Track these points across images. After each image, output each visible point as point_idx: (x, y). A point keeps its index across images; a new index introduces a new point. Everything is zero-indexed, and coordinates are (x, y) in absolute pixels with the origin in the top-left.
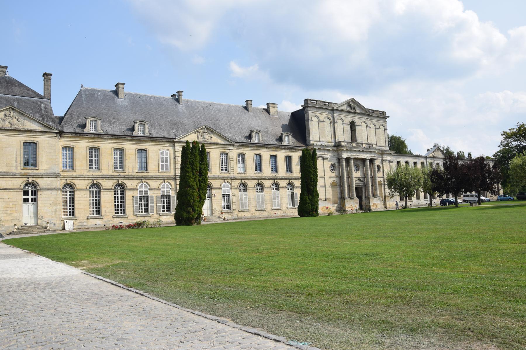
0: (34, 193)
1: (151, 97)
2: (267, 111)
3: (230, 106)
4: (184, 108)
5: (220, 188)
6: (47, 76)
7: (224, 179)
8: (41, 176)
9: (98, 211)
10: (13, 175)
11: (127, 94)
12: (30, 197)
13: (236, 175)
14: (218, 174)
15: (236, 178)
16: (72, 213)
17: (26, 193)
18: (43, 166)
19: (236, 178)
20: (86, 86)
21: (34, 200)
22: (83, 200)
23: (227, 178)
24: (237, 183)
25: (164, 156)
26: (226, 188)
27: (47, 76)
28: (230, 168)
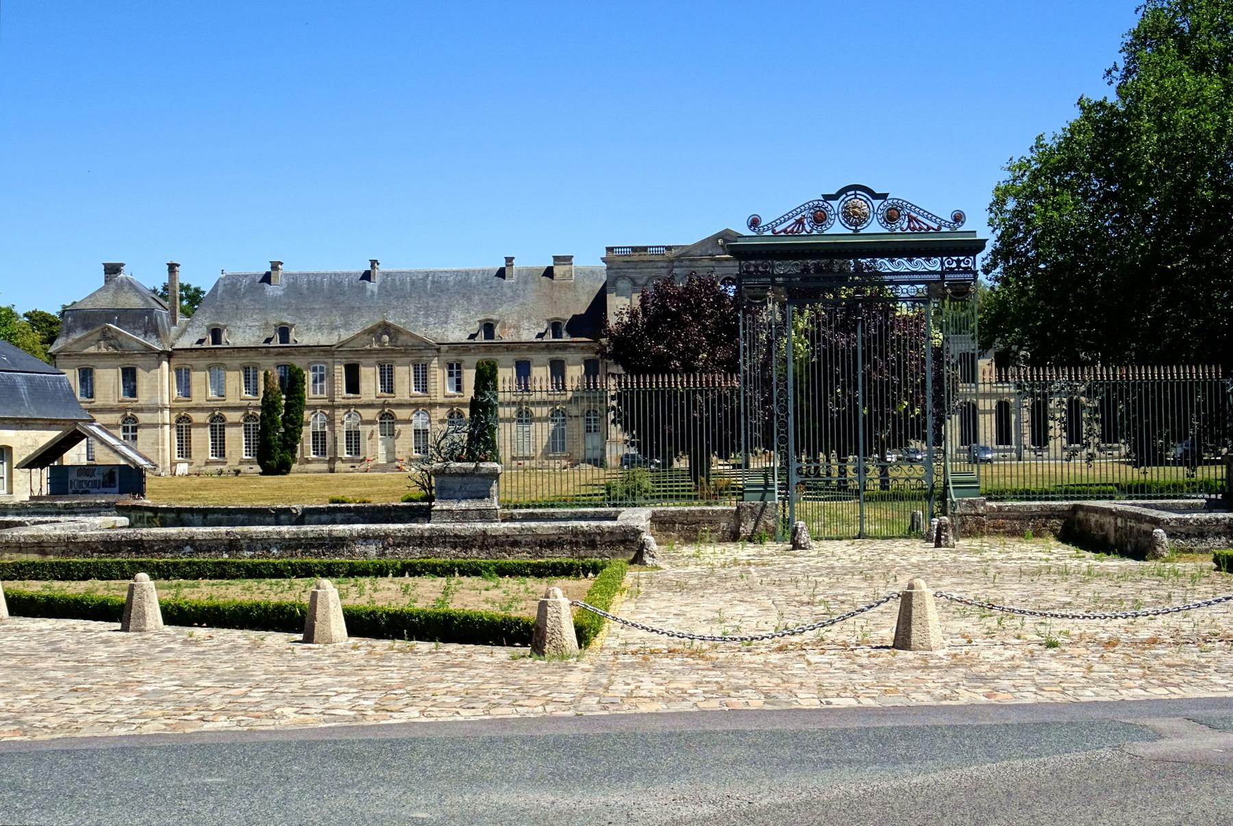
0: (135, 429)
1: (324, 275)
2: (549, 272)
3: (467, 273)
4: (376, 290)
5: (410, 421)
6: (172, 268)
7: (416, 406)
8: (141, 410)
9: (222, 455)
10: (111, 410)
11: (286, 275)
12: (130, 434)
13: (440, 399)
14: (407, 398)
15: (442, 405)
16: (188, 455)
17: (125, 430)
18: (143, 397)
19: (442, 405)
20: (228, 272)
21: (135, 438)
22: (201, 439)
23: (423, 405)
24: (441, 413)
25: (318, 373)
26: (419, 421)
27: (172, 268)
28: (431, 387)
